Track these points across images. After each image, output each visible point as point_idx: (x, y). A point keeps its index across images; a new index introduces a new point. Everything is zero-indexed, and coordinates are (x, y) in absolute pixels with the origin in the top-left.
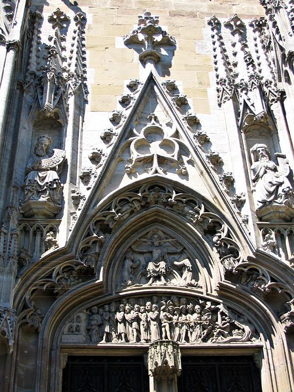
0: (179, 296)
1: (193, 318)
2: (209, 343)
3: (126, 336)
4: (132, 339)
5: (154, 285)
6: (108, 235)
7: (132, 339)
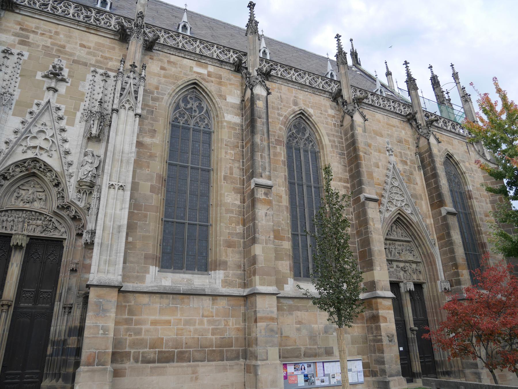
0: (36, 212)
1: (39, 222)
2: (43, 235)
3: (6, 227)
4: (9, 228)
5: (25, 206)
6: (6, 181)
7: (9, 228)
